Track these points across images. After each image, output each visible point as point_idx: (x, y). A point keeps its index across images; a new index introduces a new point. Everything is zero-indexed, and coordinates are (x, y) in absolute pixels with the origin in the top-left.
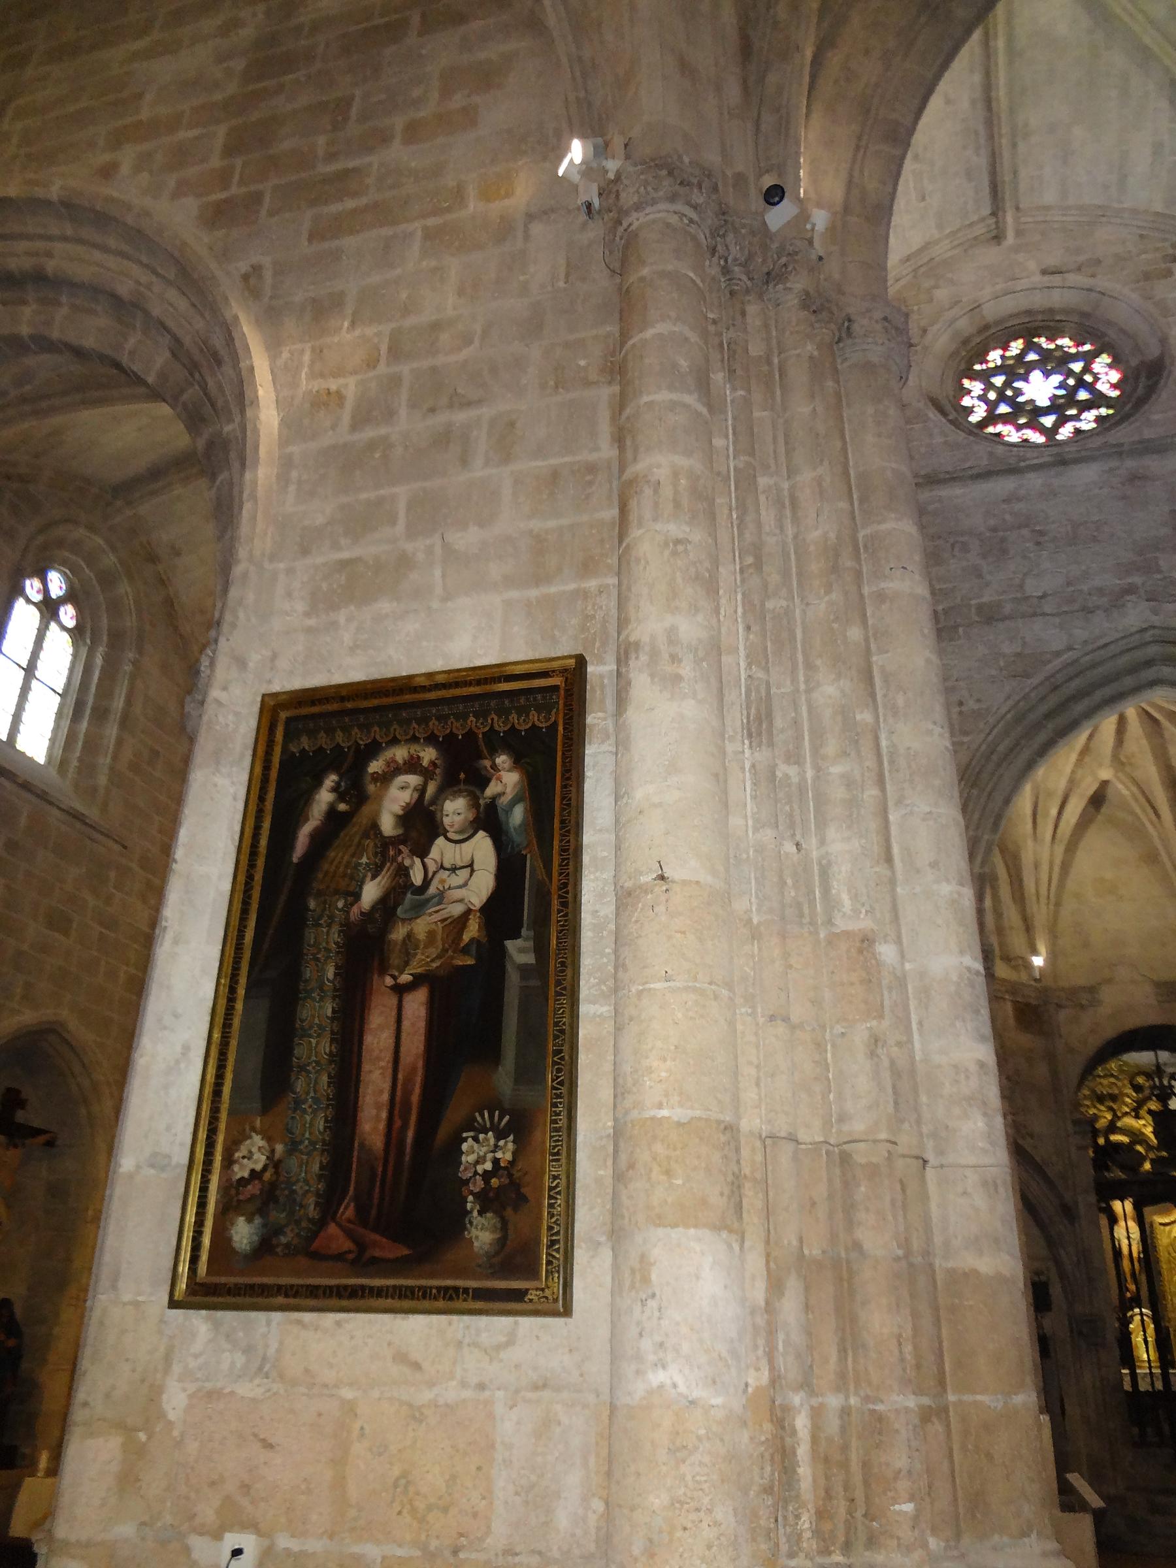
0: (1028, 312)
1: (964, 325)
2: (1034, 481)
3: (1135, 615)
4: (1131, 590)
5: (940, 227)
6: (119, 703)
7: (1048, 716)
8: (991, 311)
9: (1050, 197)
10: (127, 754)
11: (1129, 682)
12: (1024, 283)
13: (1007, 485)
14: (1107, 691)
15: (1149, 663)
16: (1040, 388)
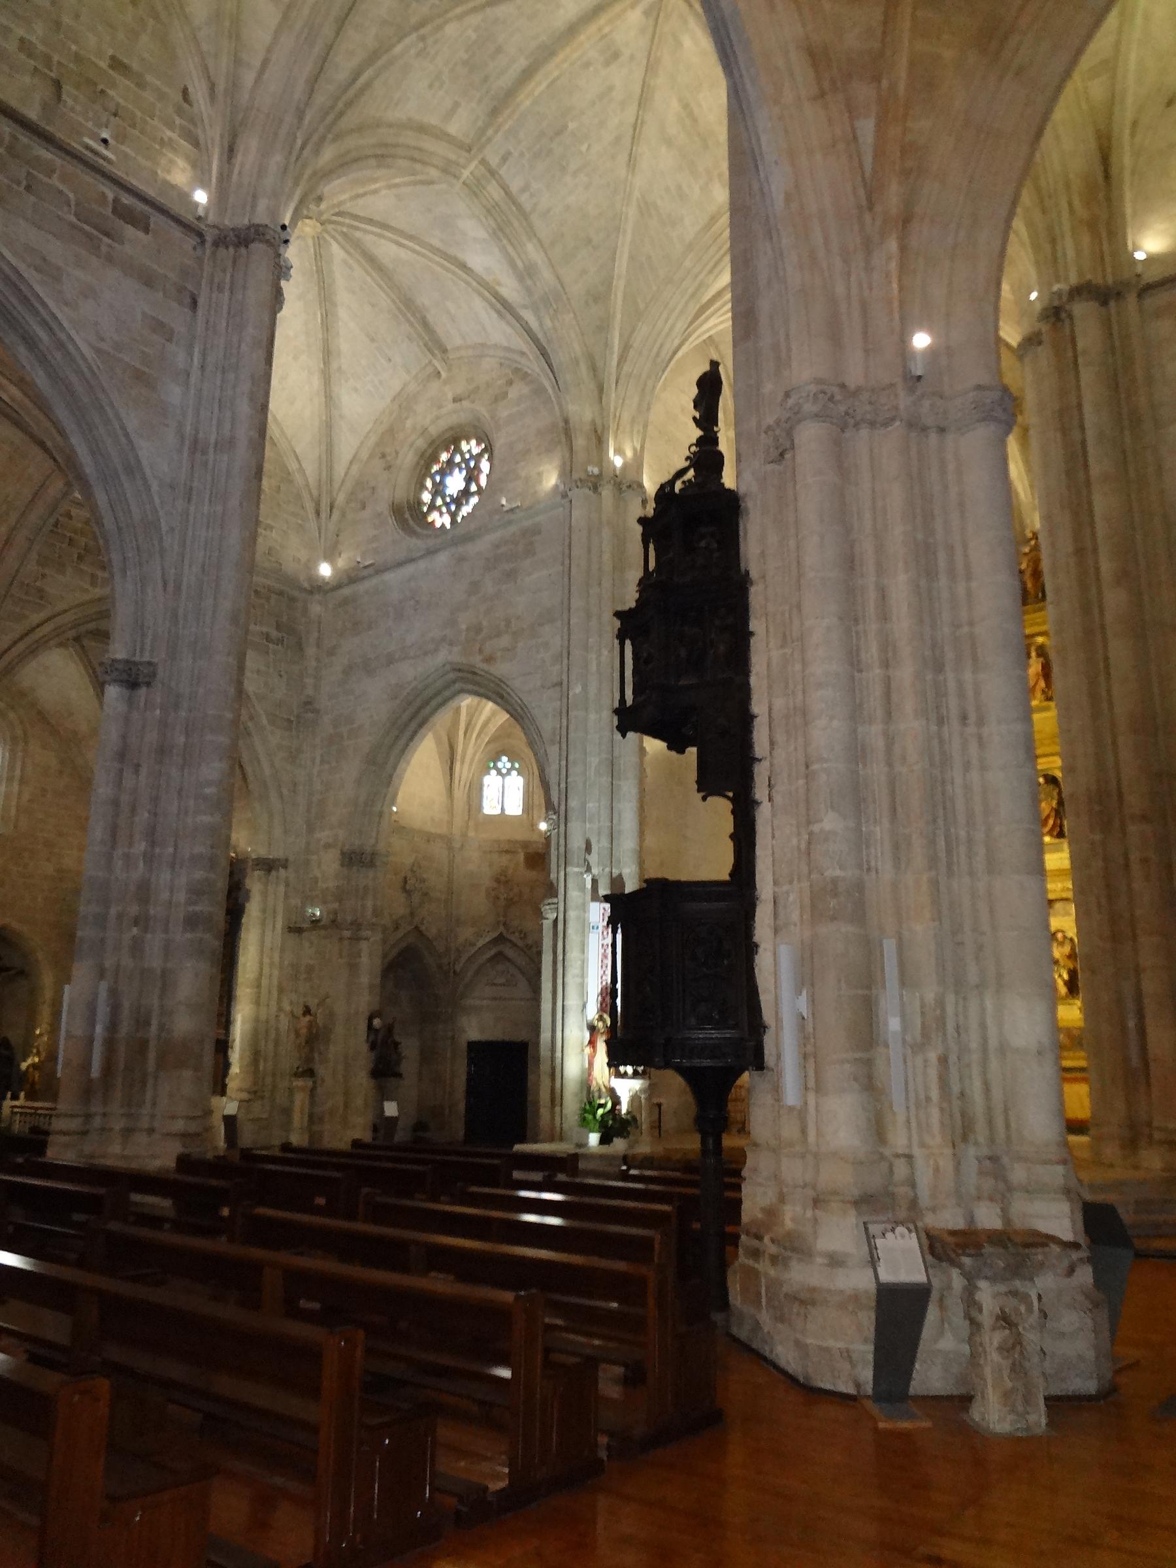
0: (451, 428)
1: (421, 443)
2: (422, 565)
3: (443, 656)
4: (443, 639)
5: (408, 372)
6: (18, 773)
7: (411, 720)
8: (434, 431)
9: (458, 341)
10: (26, 796)
11: (447, 693)
12: (444, 411)
13: (409, 569)
14: (439, 699)
15: (454, 682)
16: (455, 483)
